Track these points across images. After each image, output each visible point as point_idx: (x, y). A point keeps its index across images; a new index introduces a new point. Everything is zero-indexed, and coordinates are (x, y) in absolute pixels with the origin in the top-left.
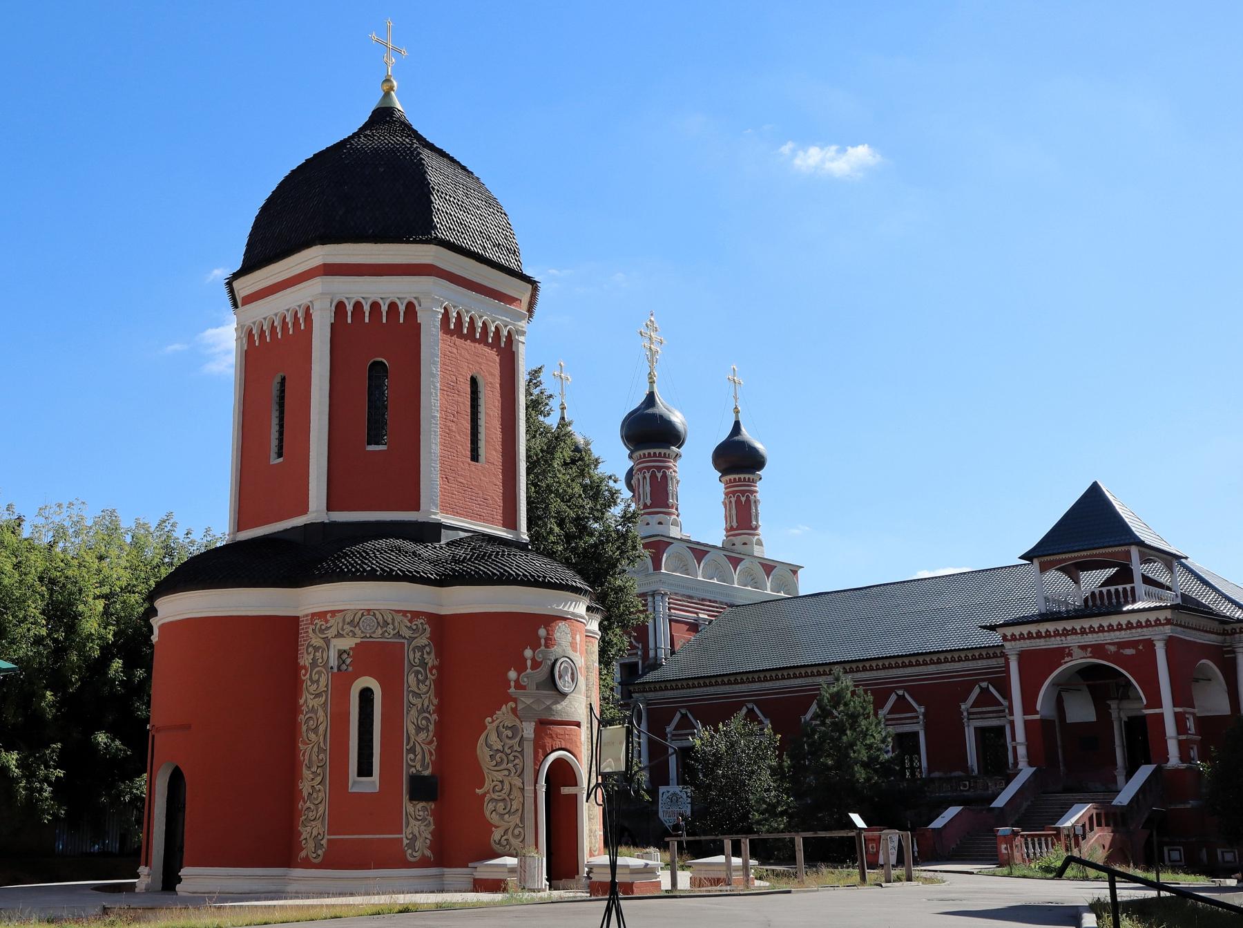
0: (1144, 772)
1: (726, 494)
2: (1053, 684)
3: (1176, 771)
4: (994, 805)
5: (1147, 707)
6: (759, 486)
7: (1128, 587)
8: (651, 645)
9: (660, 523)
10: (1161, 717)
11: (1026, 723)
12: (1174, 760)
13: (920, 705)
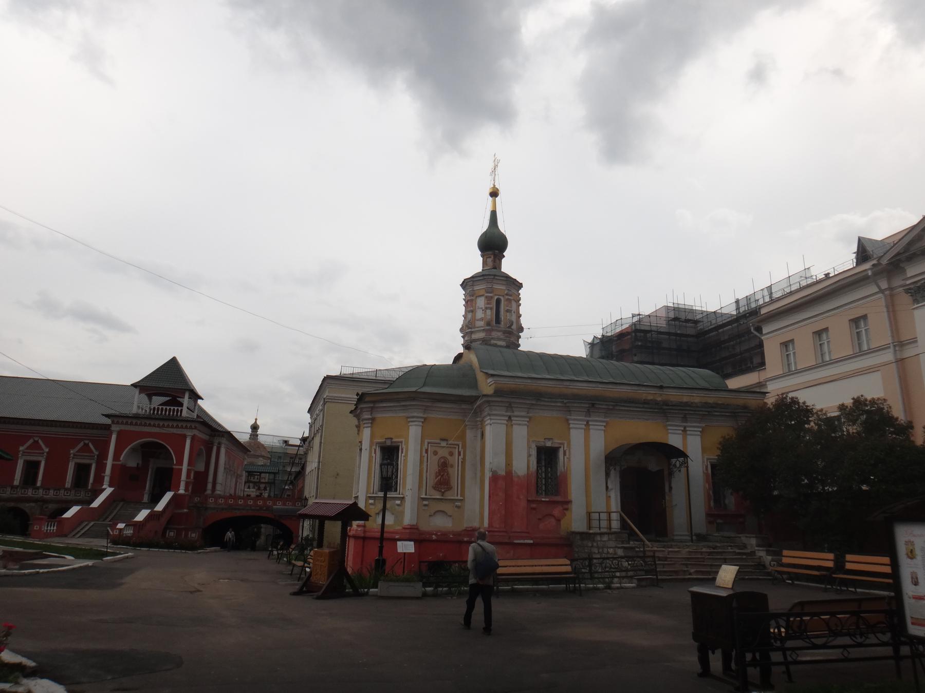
0: (168, 496)
3: (181, 495)
12: (182, 491)
13: (47, 446)
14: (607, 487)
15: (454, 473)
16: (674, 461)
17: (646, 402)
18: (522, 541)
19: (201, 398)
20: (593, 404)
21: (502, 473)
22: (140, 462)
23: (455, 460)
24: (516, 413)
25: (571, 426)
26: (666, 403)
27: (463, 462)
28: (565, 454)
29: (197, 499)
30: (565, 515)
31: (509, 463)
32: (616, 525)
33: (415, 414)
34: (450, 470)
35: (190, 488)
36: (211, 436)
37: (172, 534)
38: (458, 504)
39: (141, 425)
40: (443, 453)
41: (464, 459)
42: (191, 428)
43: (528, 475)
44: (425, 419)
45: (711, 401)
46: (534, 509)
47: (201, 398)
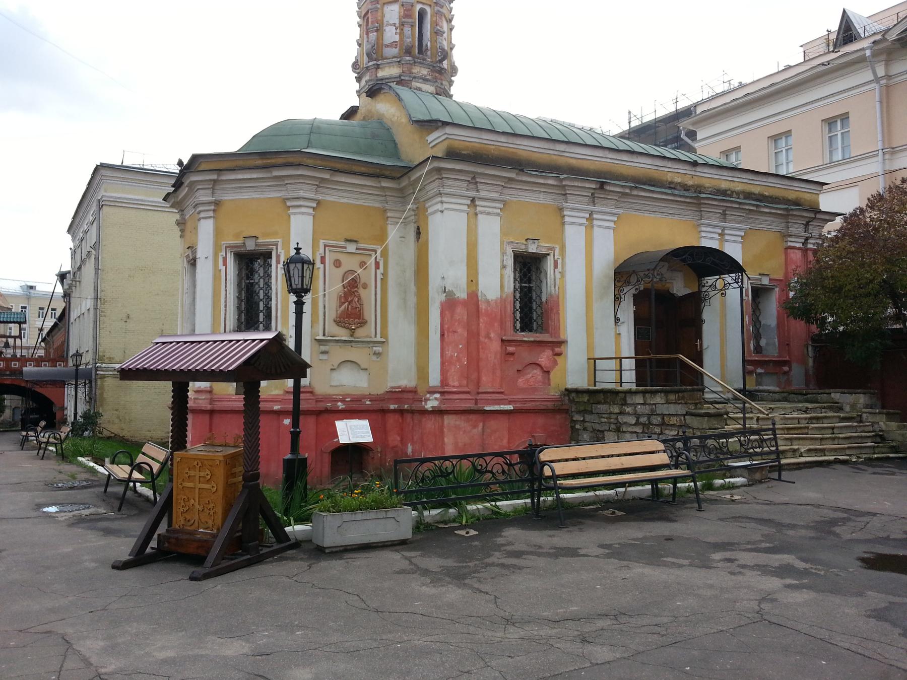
14: (617, 320)
15: (369, 298)
16: (710, 280)
17: (672, 186)
18: (496, 408)
20: (602, 185)
21: (462, 295)
23: (368, 275)
24: (483, 194)
25: (567, 219)
26: (699, 189)
27: (384, 280)
28: (556, 266)
30: (555, 363)
31: (472, 280)
32: (630, 377)
33: (302, 194)
34: (361, 291)
38: (378, 349)
40: (350, 263)
41: (385, 274)
43: (503, 300)
44: (319, 203)
45: (756, 190)
46: (512, 354)
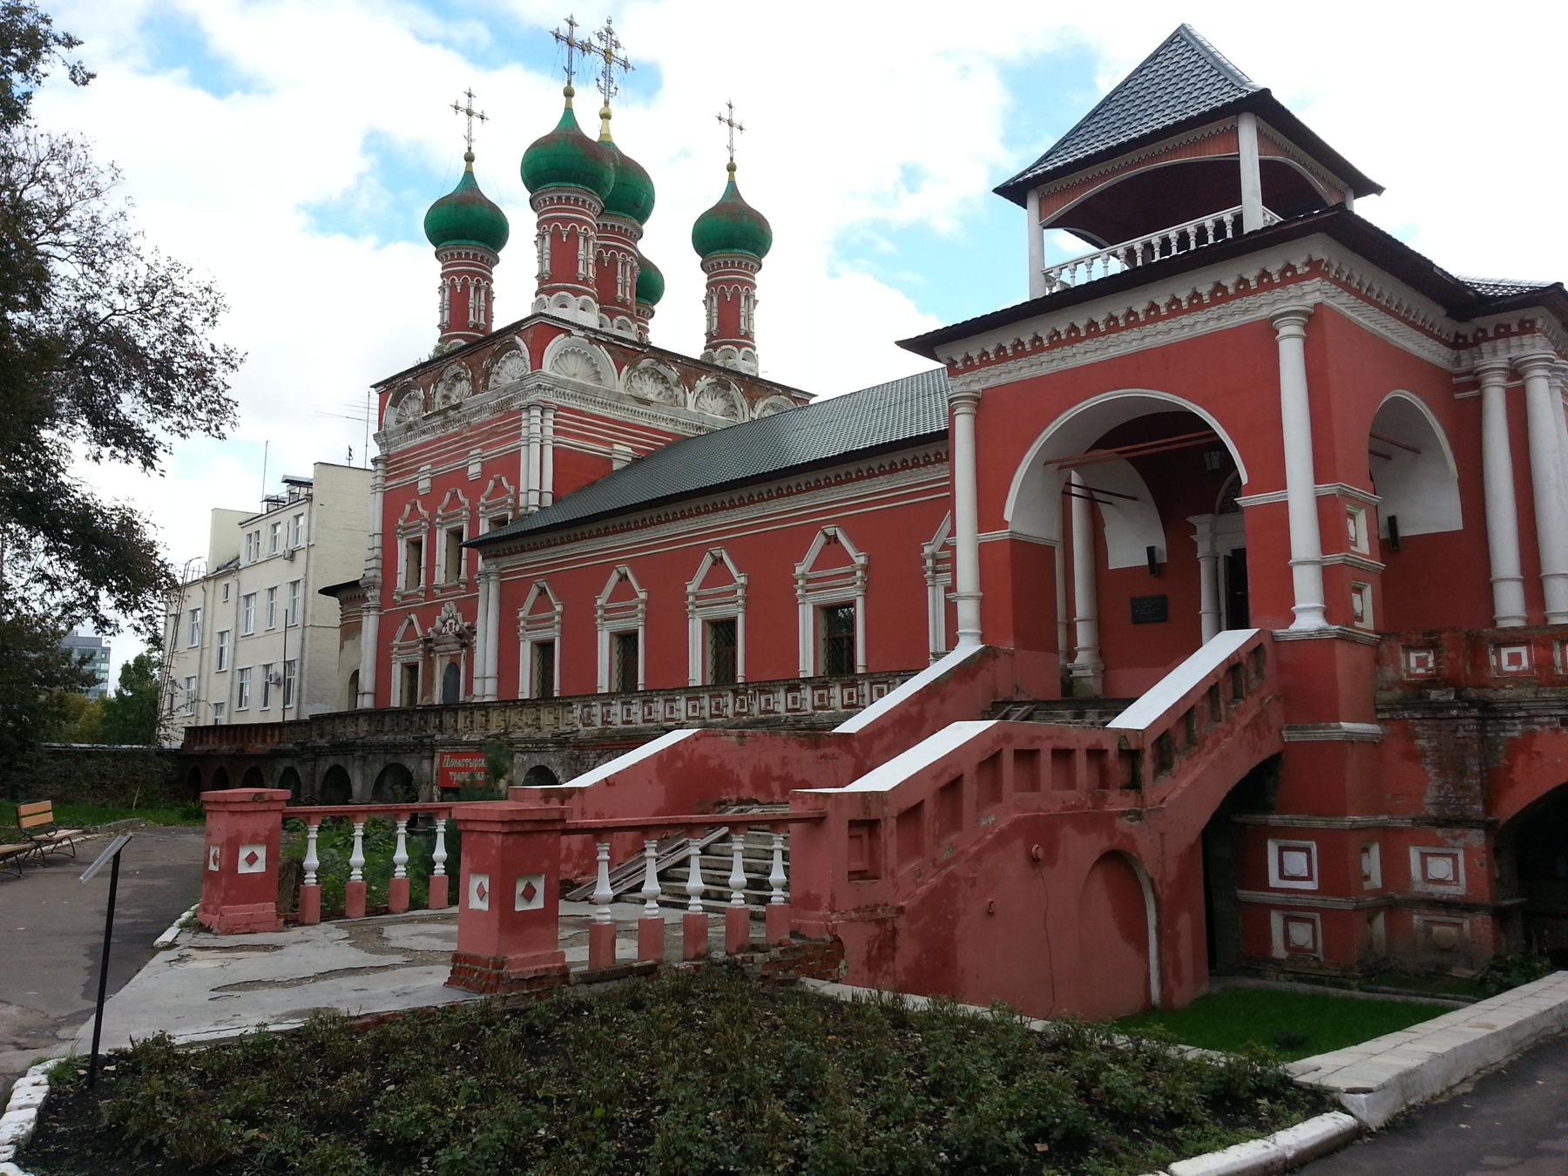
1: (708, 286)
2: (1044, 462)
4: (843, 728)
5: (1254, 488)
6: (760, 278)
7: (1227, 216)
8: (523, 489)
9: (563, 306)
10: (1279, 515)
11: (983, 550)
12: (1308, 620)
13: (859, 547)
19: (1366, 187)
22: (1161, 544)
29: (1417, 664)
35: (1364, 604)
36: (1457, 344)
37: (1297, 862)
39: (1057, 342)
42: (1290, 276)
47: (1366, 187)
